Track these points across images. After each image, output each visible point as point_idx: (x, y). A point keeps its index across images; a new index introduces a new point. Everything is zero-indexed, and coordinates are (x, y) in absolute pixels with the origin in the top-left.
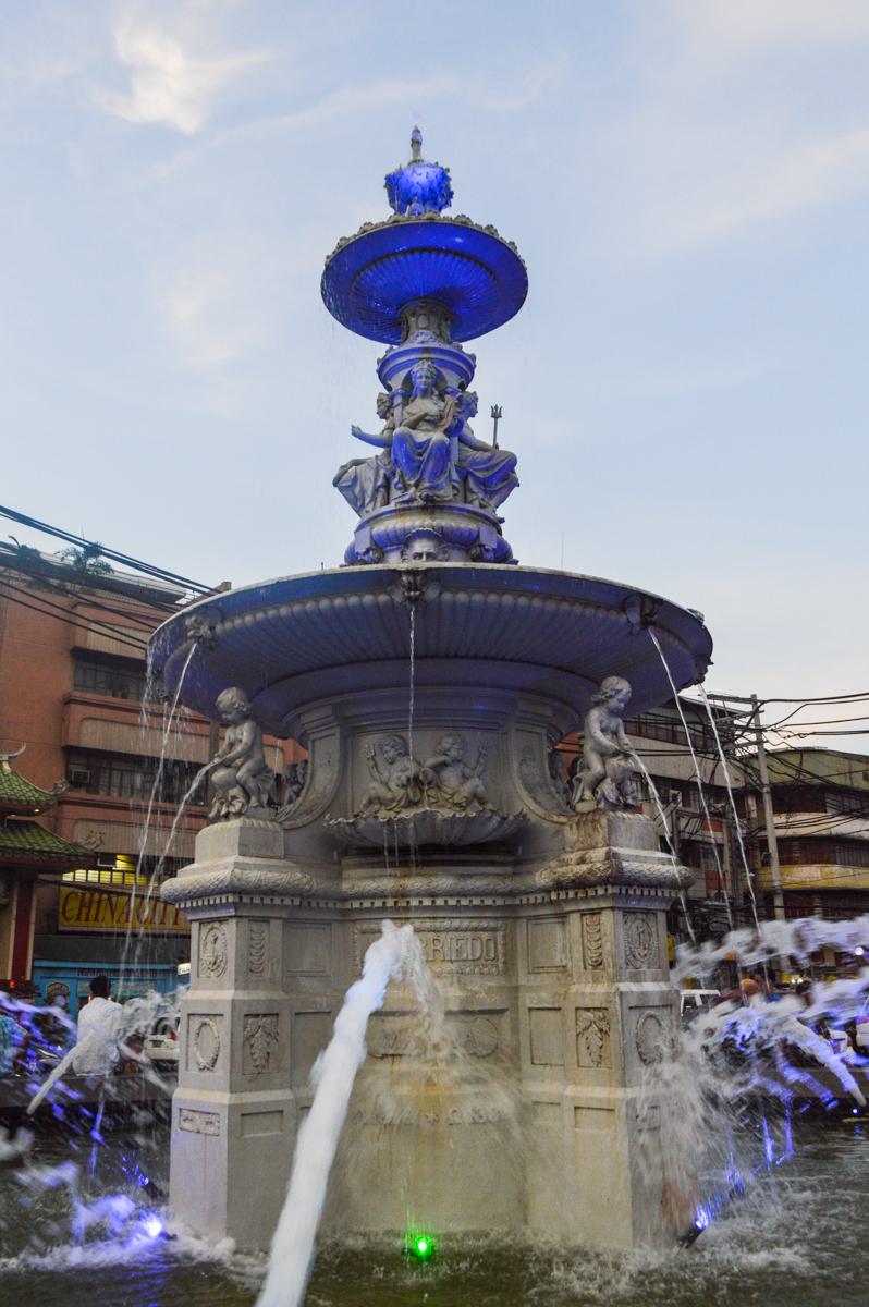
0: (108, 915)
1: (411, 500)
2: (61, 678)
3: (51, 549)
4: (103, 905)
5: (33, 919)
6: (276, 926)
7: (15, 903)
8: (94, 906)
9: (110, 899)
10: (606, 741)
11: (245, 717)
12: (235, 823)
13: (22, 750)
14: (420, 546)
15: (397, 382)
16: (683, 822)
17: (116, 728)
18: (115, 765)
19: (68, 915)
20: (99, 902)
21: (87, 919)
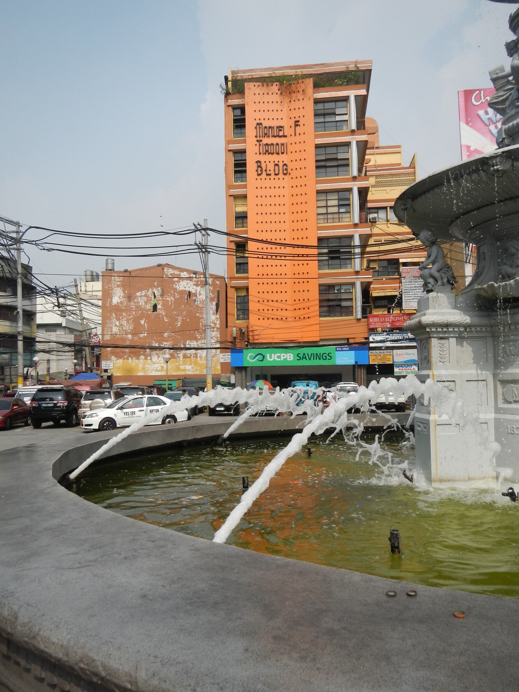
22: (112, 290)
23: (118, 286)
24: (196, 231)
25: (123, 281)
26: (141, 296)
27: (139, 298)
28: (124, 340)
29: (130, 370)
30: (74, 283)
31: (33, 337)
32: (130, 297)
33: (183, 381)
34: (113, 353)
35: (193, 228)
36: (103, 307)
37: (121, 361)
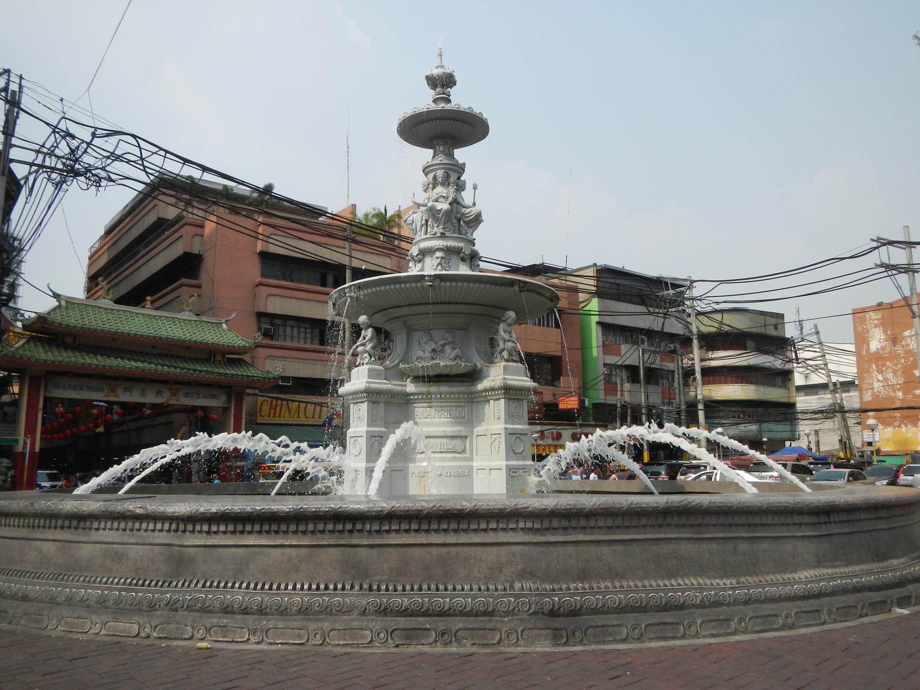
0: (287, 414)
1: (435, 234)
2: (253, 270)
3: (243, 190)
4: (284, 407)
5: (244, 416)
6: (382, 405)
7: (233, 407)
8: (278, 408)
9: (287, 404)
10: (506, 336)
11: (369, 326)
12: (366, 367)
13: (233, 316)
14: (439, 254)
15: (431, 176)
16: (646, 356)
17: (288, 301)
18: (289, 323)
19: (263, 413)
20: (281, 405)
21: (274, 416)
22: (868, 332)
23: (876, 326)
24: (875, 248)
25: (883, 319)
26: (911, 336)
27: (909, 339)
28: (892, 399)
29: (905, 442)
30: (813, 330)
31: (792, 401)
32: (894, 340)
33: (912, 456)
34: (904, 418)
35: (875, 244)
36: (858, 354)
37: (890, 430)
